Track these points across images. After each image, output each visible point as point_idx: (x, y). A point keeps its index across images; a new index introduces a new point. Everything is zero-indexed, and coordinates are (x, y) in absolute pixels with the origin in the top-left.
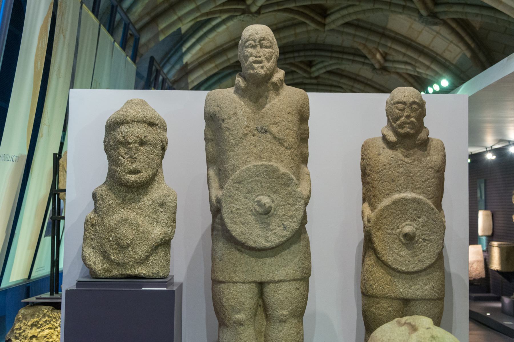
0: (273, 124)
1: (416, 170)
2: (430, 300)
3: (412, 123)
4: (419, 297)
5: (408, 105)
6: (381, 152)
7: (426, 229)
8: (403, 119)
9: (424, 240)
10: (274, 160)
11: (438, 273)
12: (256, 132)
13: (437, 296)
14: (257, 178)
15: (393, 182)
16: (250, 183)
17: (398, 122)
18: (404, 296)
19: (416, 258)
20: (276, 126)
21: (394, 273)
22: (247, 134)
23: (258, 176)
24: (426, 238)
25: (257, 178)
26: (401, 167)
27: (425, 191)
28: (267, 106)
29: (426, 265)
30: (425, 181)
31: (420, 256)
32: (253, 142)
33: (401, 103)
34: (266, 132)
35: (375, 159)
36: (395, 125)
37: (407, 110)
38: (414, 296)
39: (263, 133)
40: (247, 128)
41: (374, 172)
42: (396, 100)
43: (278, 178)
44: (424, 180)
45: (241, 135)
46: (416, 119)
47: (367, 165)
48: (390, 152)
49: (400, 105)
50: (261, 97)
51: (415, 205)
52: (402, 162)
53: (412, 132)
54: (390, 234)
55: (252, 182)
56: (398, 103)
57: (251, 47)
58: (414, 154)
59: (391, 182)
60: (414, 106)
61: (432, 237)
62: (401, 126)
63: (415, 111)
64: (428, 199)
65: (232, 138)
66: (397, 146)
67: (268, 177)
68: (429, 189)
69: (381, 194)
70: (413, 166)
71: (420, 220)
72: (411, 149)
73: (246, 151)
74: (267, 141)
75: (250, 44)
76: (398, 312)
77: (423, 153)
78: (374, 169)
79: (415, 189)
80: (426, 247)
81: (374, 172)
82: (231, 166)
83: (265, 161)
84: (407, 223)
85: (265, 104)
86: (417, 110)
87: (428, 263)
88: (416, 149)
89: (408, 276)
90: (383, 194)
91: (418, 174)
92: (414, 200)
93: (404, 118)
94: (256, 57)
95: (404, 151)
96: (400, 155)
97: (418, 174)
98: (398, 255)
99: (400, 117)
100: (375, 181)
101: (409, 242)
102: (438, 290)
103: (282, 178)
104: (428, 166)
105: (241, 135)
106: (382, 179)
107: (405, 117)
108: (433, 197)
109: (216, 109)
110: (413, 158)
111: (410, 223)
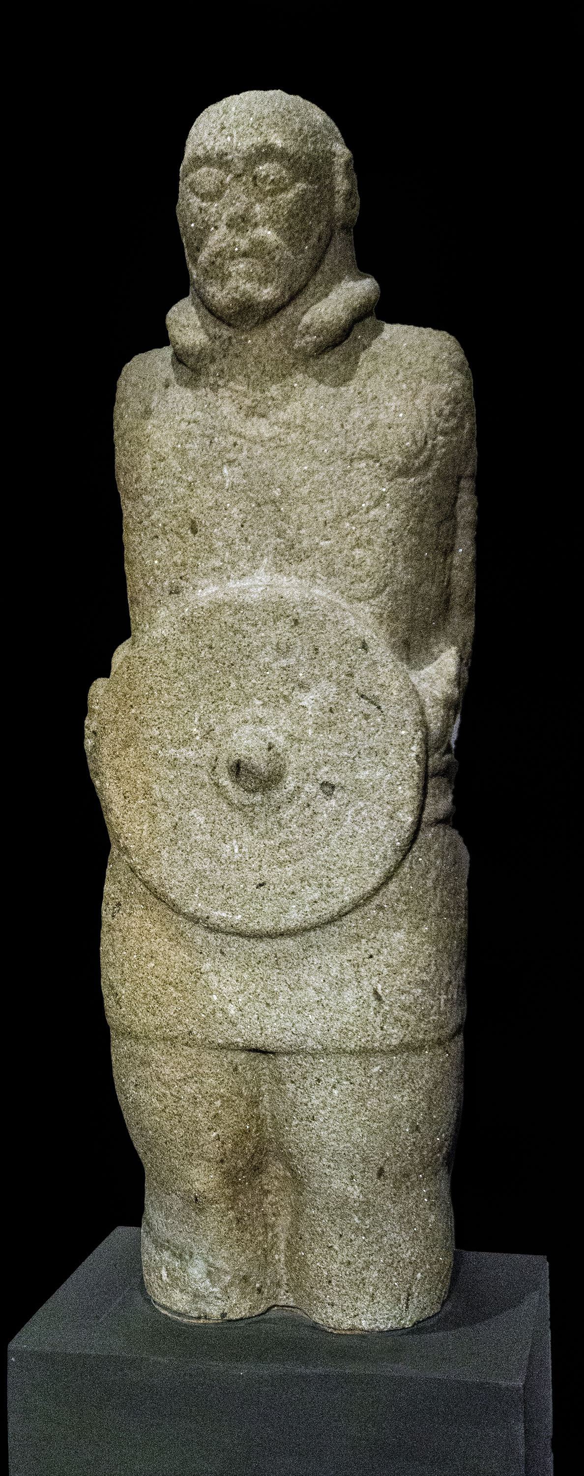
1: (297, 470)
2: (365, 1053)
3: (257, 250)
4: (310, 1043)
7: (335, 738)
9: (328, 788)
11: (400, 935)
13: (396, 1035)
15: (194, 531)
18: (249, 1031)
19: (289, 870)
21: (199, 935)
24: (335, 779)
26: (230, 462)
27: (339, 566)
29: (334, 906)
30: (338, 518)
31: (308, 861)
37: (238, 189)
38: (288, 1037)
44: (330, 514)
46: (278, 231)
51: (283, 631)
52: (232, 439)
53: (267, 293)
54: (173, 764)
58: (287, 398)
59: (186, 531)
60: (263, 169)
61: (363, 775)
63: (273, 193)
64: (351, 599)
66: (213, 368)
68: (358, 553)
70: (282, 454)
71: (307, 699)
72: (274, 378)
76: (227, 1102)
77: (332, 390)
79: (290, 554)
80: (337, 819)
84: (247, 713)
86: (279, 187)
87: (348, 891)
88: (300, 377)
89: (262, 948)
91: (304, 491)
92: (278, 610)
93: (223, 229)
97: (304, 491)
98: (211, 853)
101: (258, 798)
102: (404, 1008)
104: (350, 449)
108: (378, 592)
110: (282, 416)
111: (260, 712)
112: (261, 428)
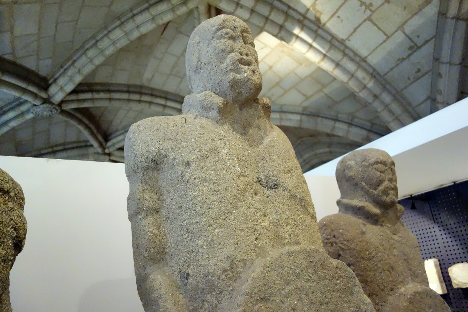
0: (285, 172)
5: (389, 166)
6: (364, 230)
8: (386, 183)
10: (302, 241)
12: (257, 187)
14: (299, 284)
16: (287, 297)
17: (381, 188)
20: (290, 175)
22: (245, 190)
23: (298, 276)
25: (299, 284)
26: (394, 248)
28: (266, 141)
32: (259, 206)
33: (381, 163)
34: (276, 186)
35: (360, 240)
36: (376, 192)
39: (271, 188)
40: (242, 178)
41: (363, 258)
42: (372, 160)
43: (333, 277)
45: (235, 192)
47: (343, 250)
48: (375, 228)
49: (379, 165)
50: (250, 125)
55: (290, 293)
56: (377, 163)
57: (229, 38)
62: (385, 192)
65: (215, 198)
67: (315, 277)
69: (383, 290)
73: (250, 224)
74: (283, 205)
75: (227, 33)
78: (362, 255)
81: (363, 258)
82: (221, 261)
83: (289, 244)
85: (262, 138)
90: (385, 290)
94: (241, 54)
95: (390, 226)
96: (388, 232)
99: (383, 181)
100: (370, 271)
103: (340, 277)
105: (235, 192)
106: (379, 268)
107: (388, 180)
109: (168, 145)
112: (396, 237)
